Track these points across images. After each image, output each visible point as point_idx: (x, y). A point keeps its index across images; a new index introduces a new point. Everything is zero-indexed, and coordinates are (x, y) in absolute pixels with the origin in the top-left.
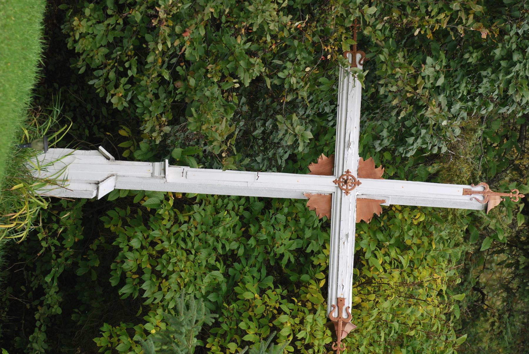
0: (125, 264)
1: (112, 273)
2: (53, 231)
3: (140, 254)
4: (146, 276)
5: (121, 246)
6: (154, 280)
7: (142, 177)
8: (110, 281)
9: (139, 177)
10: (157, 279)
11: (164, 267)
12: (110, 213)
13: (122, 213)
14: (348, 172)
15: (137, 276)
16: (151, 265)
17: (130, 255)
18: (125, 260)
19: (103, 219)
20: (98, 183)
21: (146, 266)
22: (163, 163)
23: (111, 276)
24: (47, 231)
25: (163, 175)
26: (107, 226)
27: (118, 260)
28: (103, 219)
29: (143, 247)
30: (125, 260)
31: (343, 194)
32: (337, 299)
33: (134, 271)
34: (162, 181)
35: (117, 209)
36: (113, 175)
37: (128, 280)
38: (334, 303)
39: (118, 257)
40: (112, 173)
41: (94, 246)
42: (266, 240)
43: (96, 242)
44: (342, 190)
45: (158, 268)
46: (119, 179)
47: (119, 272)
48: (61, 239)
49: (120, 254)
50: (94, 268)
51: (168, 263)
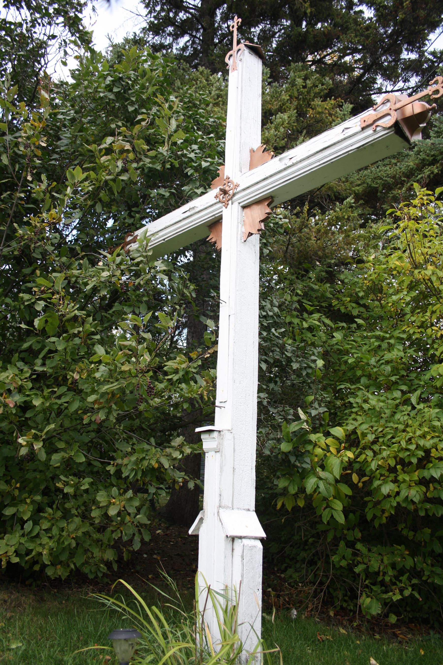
0: (414, 500)
1: (431, 514)
2: (394, 580)
3: (403, 482)
4: (426, 474)
5: (395, 504)
6: (431, 465)
7: (221, 468)
8: (440, 515)
9: (221, 471)
10: (431, 462)
11: (414, 455)
12: (369, 517)
13: (370, 505)
14: (216, 197)
15: (431, 485)
16: (415, 471)
17: (403, 494)
18: (409, 499)
19: (377, 524)
20: (233, 539)
21: (416, 476)
22: (203, 437)
23: (434, 514)
24: (394, 587)
25: (215, 434)
26: (384, 521)
27: (411, 507)
28: (377, 524)
29: (395, 481)
30: (409, 499)
31: (239, 189)
32: (363, 129)
33: (424, 489)
34: (227, 436)
35: (367, 510)
36: (218, 512)
37: (436, 496)
38: (370, 131)
39: (408, 508)
40: (216, 514)
41: (411, 534)
42: (391, 367)
43: (405, 532)
44: (234, 195)
45: (414, 461)
46: (227, 501)
47: (428, 506)
48: (402, 572)
49: (404, 505)
50: (432, 535)
51: (407, 450)
